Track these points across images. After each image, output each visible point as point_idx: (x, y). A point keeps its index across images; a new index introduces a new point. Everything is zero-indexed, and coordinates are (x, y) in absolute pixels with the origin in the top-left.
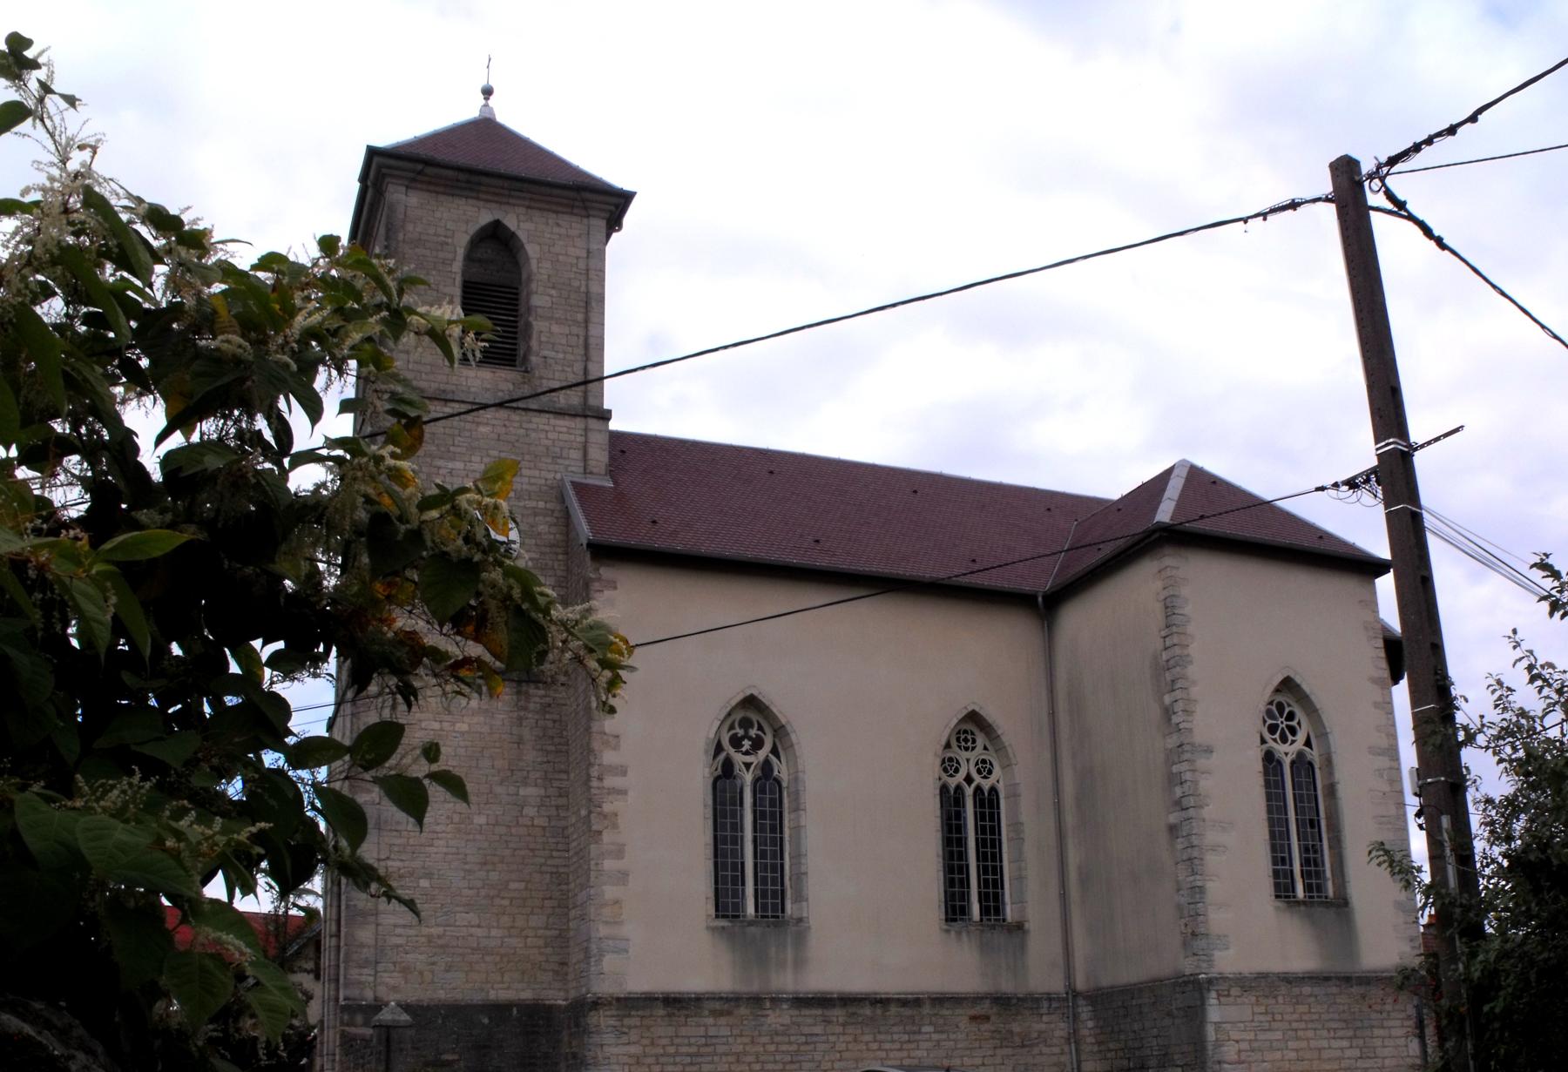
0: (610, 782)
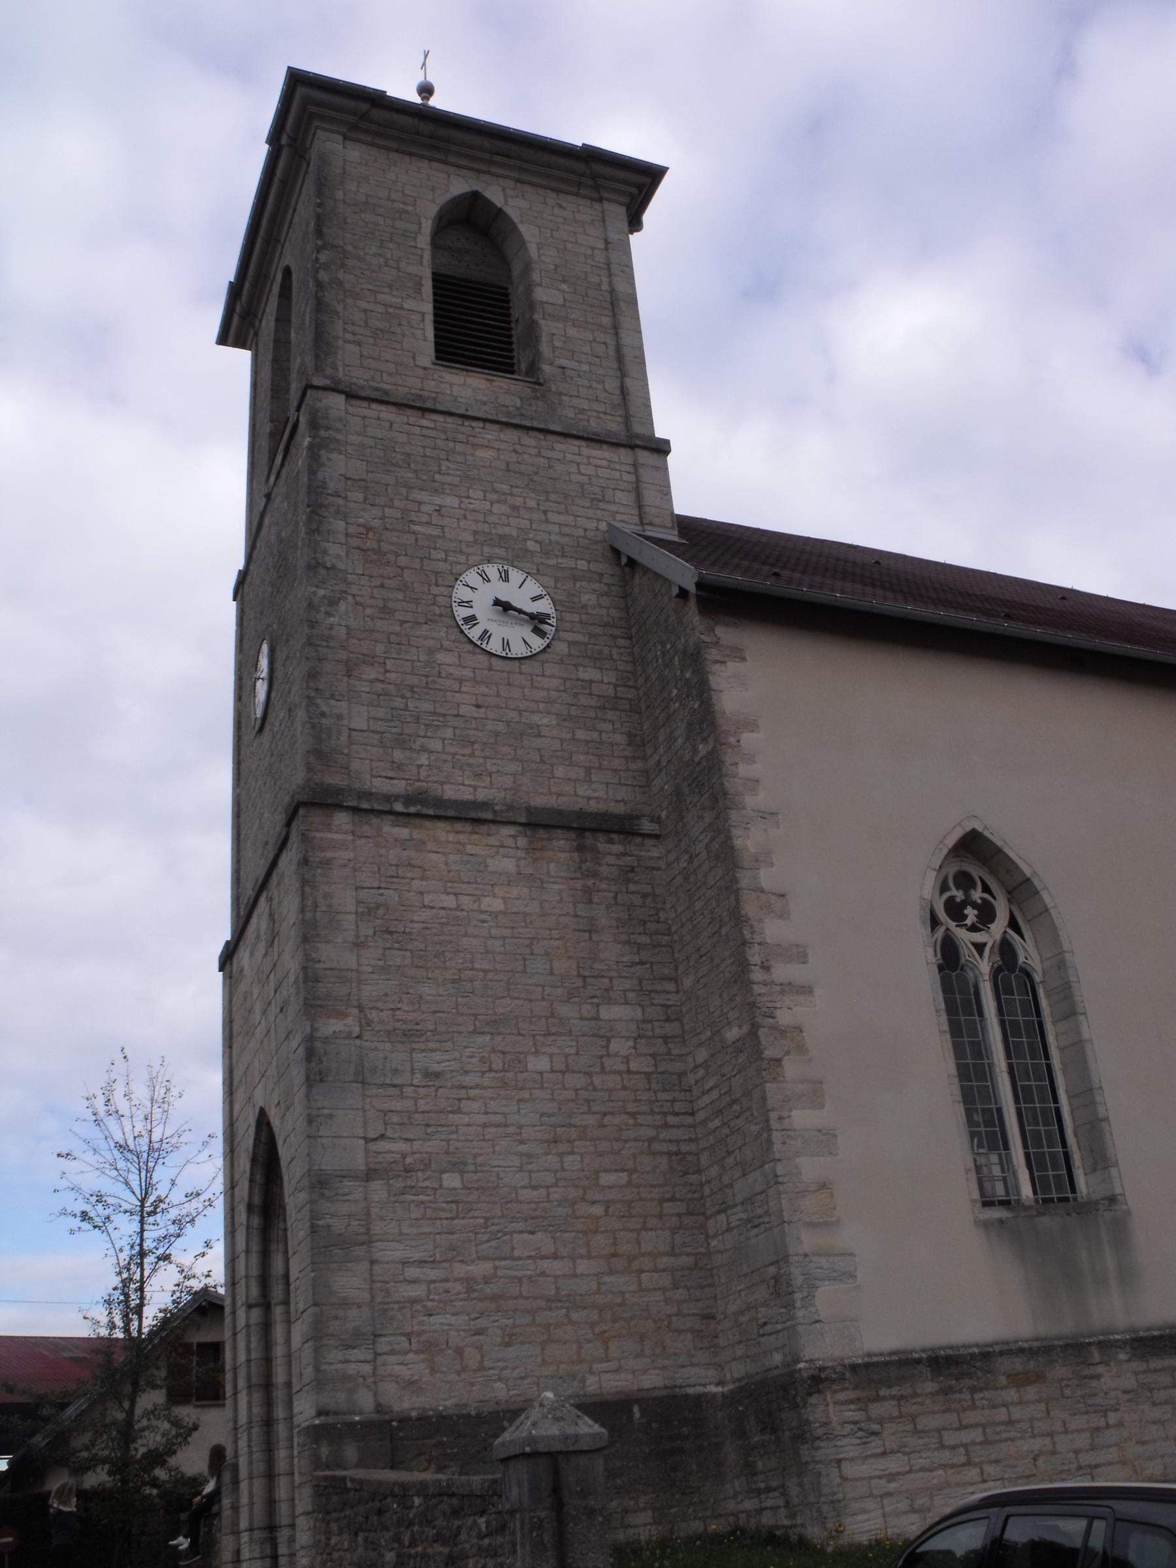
0: (783, 972)
